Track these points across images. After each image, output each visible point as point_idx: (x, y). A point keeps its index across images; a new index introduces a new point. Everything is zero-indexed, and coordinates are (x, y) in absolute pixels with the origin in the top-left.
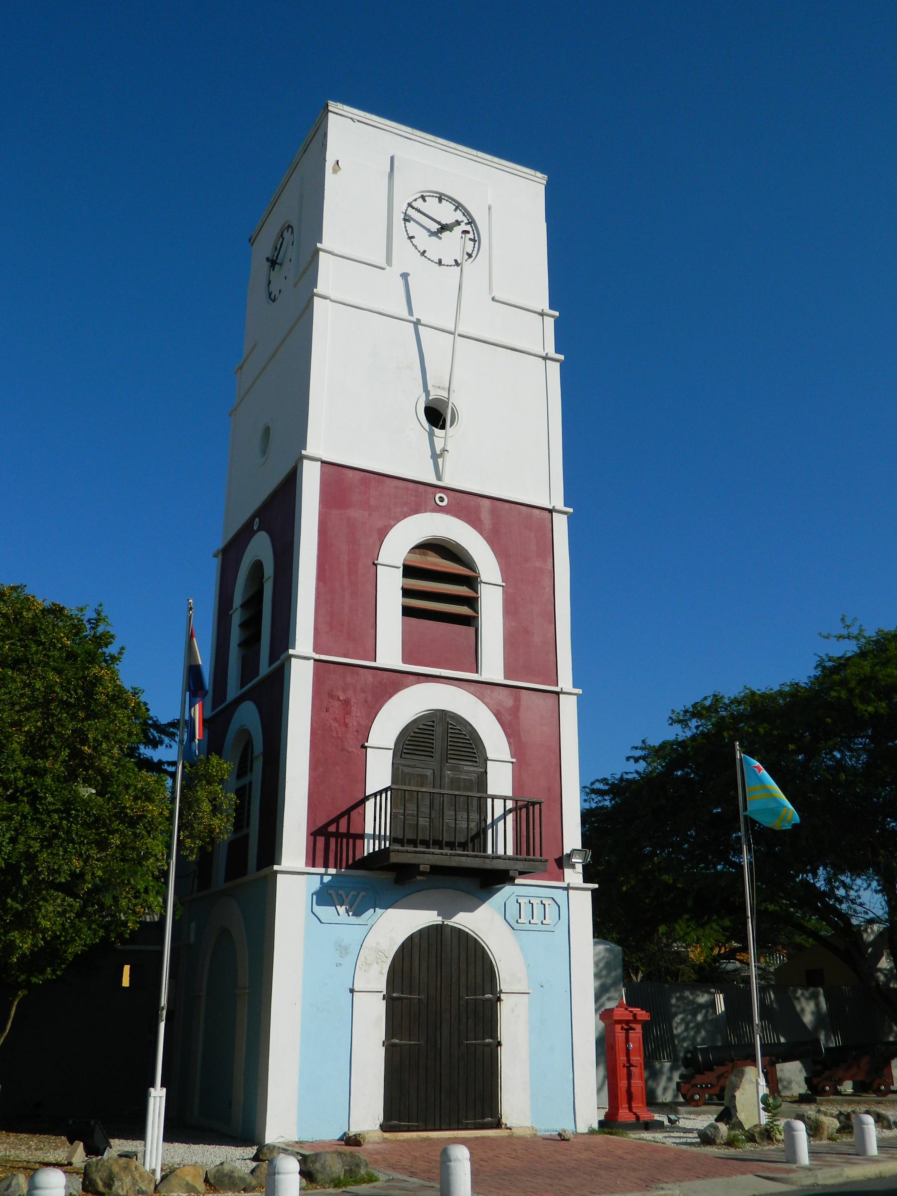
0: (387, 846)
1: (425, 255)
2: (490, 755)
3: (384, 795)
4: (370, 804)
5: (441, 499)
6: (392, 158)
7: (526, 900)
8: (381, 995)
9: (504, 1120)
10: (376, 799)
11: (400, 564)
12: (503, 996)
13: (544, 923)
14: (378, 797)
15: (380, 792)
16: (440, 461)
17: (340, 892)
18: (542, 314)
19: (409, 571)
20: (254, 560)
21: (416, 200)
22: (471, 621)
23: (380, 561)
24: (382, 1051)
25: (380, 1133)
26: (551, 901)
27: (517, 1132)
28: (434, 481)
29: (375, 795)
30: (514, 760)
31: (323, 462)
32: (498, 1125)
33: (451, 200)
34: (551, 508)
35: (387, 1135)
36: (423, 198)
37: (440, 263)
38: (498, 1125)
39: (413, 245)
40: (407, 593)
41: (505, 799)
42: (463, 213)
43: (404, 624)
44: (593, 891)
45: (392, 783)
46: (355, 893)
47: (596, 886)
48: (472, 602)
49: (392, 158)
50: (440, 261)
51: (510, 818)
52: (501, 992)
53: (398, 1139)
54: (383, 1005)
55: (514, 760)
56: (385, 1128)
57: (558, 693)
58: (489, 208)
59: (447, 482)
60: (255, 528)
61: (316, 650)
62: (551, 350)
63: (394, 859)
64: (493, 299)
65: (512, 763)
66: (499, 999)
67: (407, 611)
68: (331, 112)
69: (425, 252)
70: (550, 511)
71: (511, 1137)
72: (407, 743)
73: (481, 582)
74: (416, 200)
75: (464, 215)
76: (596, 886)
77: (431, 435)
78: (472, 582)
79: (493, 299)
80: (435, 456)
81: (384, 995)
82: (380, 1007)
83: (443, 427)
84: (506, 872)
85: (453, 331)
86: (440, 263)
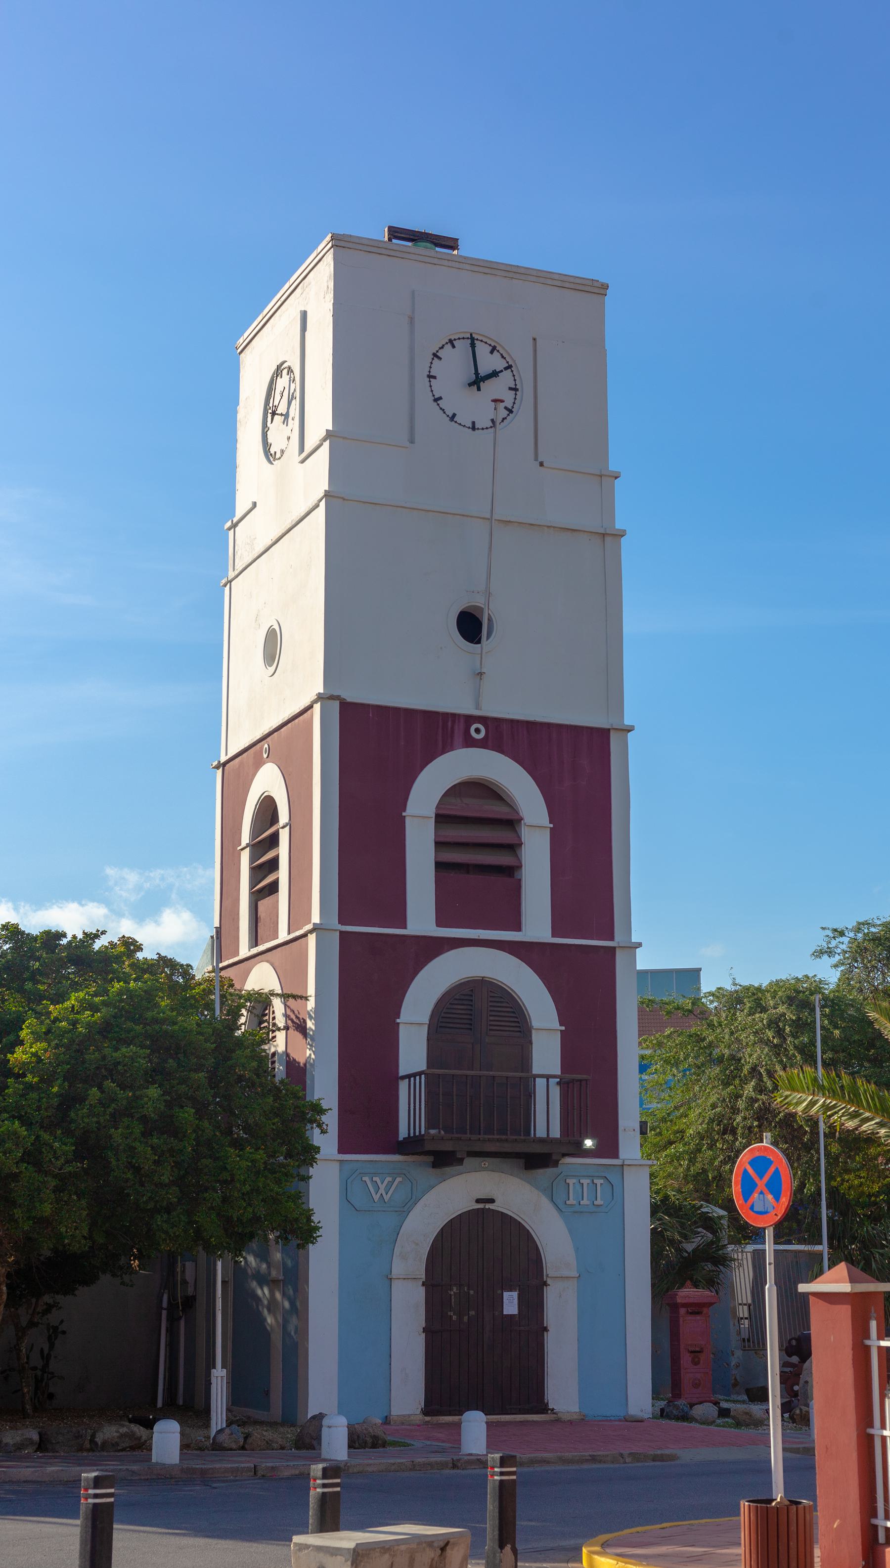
0: (423, 1133)
1: (455, 420)
2: (536, 1022)
3: (418, 1078)
4: (403, 1086)
5: (478, 731)
7: (574, 1181)
8: (421, 1283)
9: (550, 1407)
10: (410, 1082)
11: (431, 812)
12: (549, 1281)
13: (595, 1203)
14: (412, 1079)
15: (414, 1075)
17: (374, 1179)
19: (442, 819)
20: (265, 794)
21: (442, 348)
24: (421, 1339)
25: (421, 1417)
26: (602, 1181)
29: (408, 1077)
30: (563, 1028)
35: (428, 1418)
36: (451, 341)
37: (474, 428)
38: (543, 1408)
39: (441, 409)
40: (439, 845)
41: (548, 1077)
42: (502, 355)
45: (428, 1067)
46: (390, 1179)
48: (513, 848)
50: (474, 423)
52: (547, 1276)
53: (439, 1422)
54: (422, 1290)
55: (563, 1028)
56: (426, 1412)
57: (614, 948)
58: (534, 339)
60: (265, 756)
63: (429, 1147)
64: (541, 464)
65: (561, 1031)
66: (545, 1284)
67: (440, 866)
69: (454, 415)
70: (609, 730)
72: (443, 1015)
73: (525, 824)
74: (442, 348)
75: (503, 357)
78: (512, 823)
79: (541, 464)
81: (423, 1282)
82: (419, 1294)
83: (479, 642)
84: (549, 1155)
85: (488, 516)
86: (474, 428)
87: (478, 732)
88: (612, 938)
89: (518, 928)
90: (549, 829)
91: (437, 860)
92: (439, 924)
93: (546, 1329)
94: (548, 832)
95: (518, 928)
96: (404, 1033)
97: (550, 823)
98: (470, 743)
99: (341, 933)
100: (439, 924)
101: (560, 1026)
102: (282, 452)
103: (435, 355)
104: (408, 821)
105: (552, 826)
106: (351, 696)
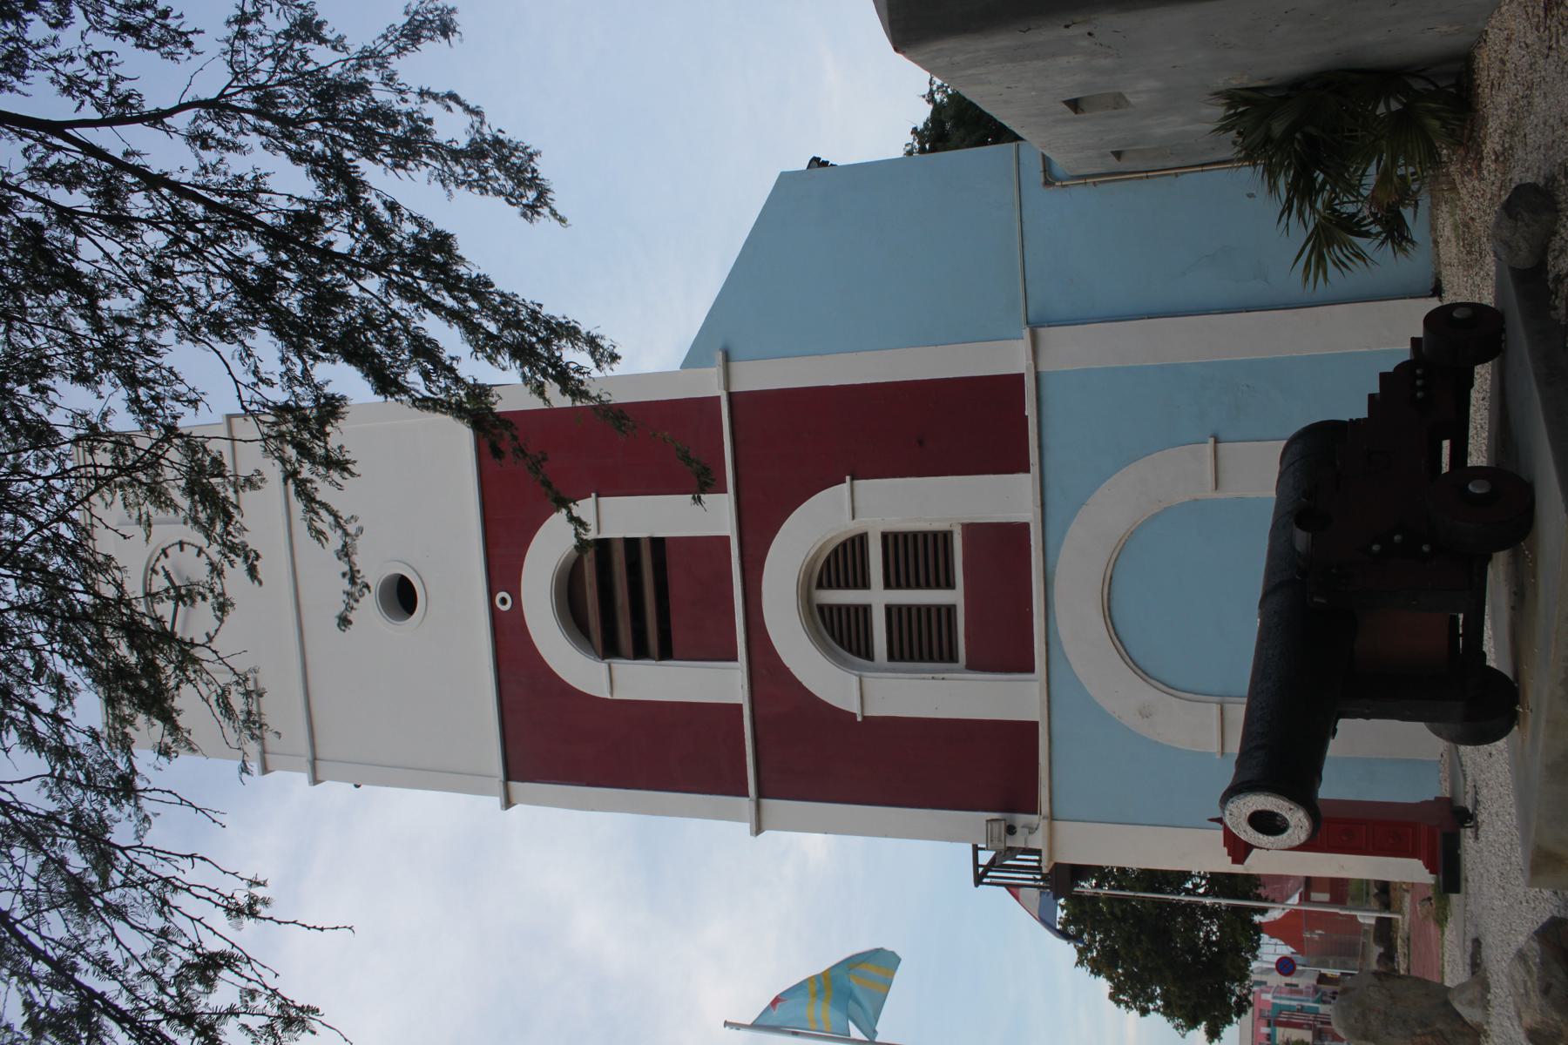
5: (504, 601)
19: (609, 649)
22: (658, 544)
30: (848, 478)
40: (640, 652)
48: (632, 544)
55: (848, 478)
57: (731, 396)
61: (744, 793)
67: (666, 653)
88: (718, 399)
89: (728, 538)
90: (601, 499)
92: (735, 659)
95: (728, 538)
96: (880, 707)
100: (735, 659)
101: (845, 482)
104: (617, 696)
105: (593, 495)
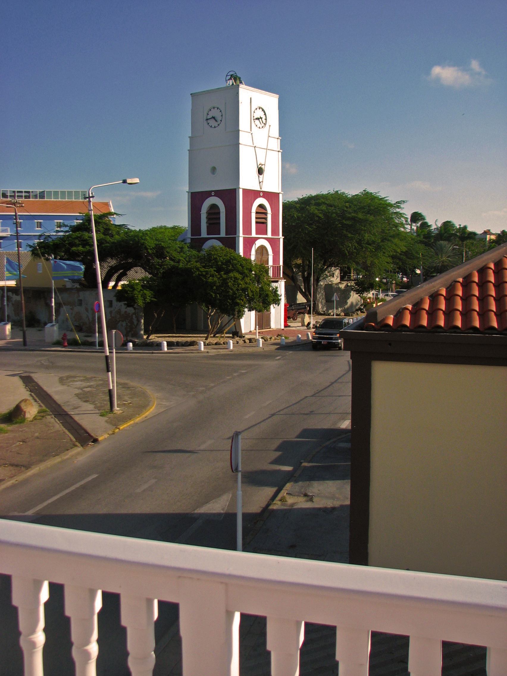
6: (251, 98)
16: (261, 184)
18: (278, 139)
19: (257, 213)
23: (252, 212)
27: (274, 329)
28: (259, 190)
31: (243, 189)
32: (270, 328)
33: (262, 108)
34: (279, 192)
38: (270, 328)
40: (256, 218)
43: (256, 225)
44: (285, 281)
47: (285, 280)
48: (266, 219)
49: (251, 98)
51: (271, 268)
59: (263, 190)
62: (279, 149)
67: (257, 223)
68: (241, 87)
70: (279, 193)
71: (273, 330)
76: (285, 280)
77: (259, 177)
78: (266, 214)
80: (260, 183)
87: (261, 194)
91: (256, 221)
93: (271, 313)
94: (271, 215)
95: (266, 234)
97: (271, 213)
98: (260, 197)
99: (244, 237)
102: (215, 127)
103: (254, 112)
106: (244, 188)
